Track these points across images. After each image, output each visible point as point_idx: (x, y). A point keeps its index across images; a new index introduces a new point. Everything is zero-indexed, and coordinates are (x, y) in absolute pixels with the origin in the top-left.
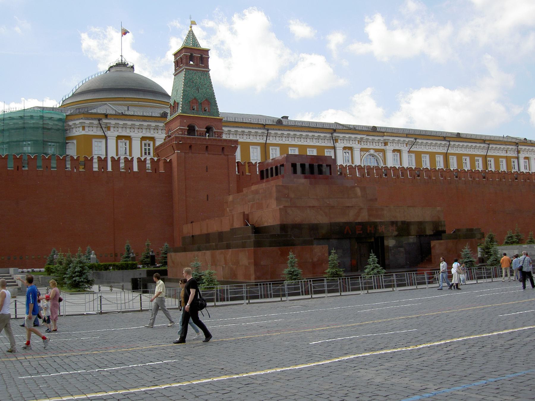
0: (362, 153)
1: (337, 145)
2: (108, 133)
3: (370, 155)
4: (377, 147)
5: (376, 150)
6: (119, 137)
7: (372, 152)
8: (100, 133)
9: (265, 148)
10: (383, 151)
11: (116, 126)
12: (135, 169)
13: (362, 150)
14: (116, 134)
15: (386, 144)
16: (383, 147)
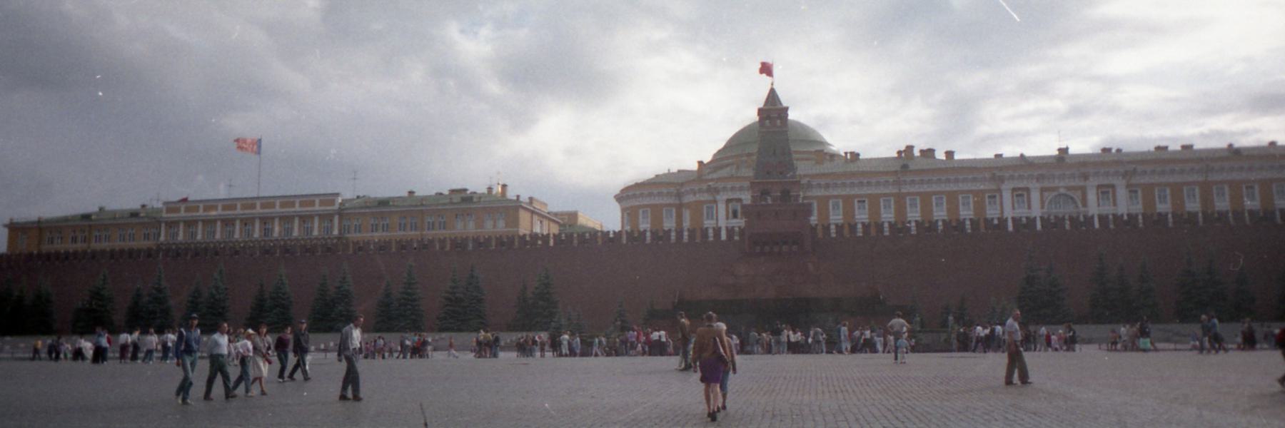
0: (1046, 194)
1: (1003, 187)
2: (718, 197)
3: (1060, 195)
4: (1073, 184)
5: (1069, 188)
6: (728, 201)
7: (1062, 191)
8: (711, 198)
9: (900, 198)
10: (1083, 190)
11: (724, 189)
12: (724, 236)
13: (1043, 190)
14: (725, 197)
15: (1086, 177)
16: (1082, 184)
